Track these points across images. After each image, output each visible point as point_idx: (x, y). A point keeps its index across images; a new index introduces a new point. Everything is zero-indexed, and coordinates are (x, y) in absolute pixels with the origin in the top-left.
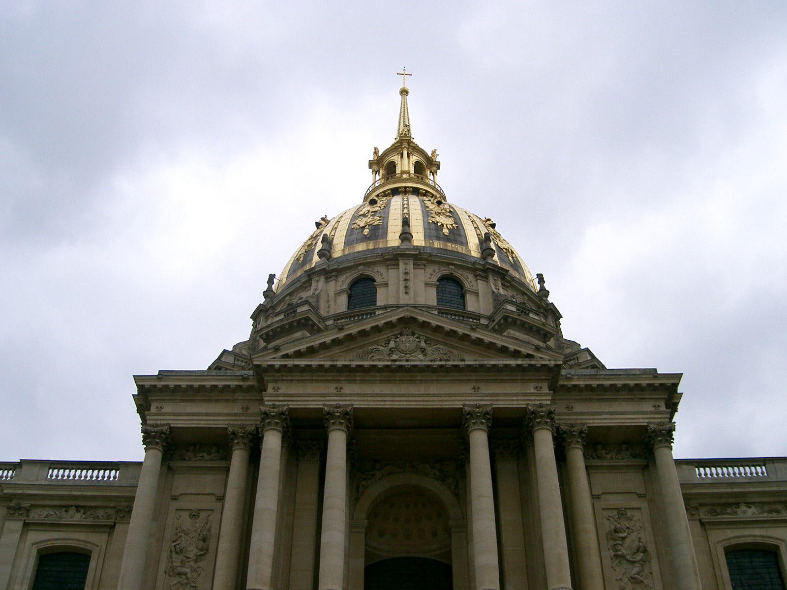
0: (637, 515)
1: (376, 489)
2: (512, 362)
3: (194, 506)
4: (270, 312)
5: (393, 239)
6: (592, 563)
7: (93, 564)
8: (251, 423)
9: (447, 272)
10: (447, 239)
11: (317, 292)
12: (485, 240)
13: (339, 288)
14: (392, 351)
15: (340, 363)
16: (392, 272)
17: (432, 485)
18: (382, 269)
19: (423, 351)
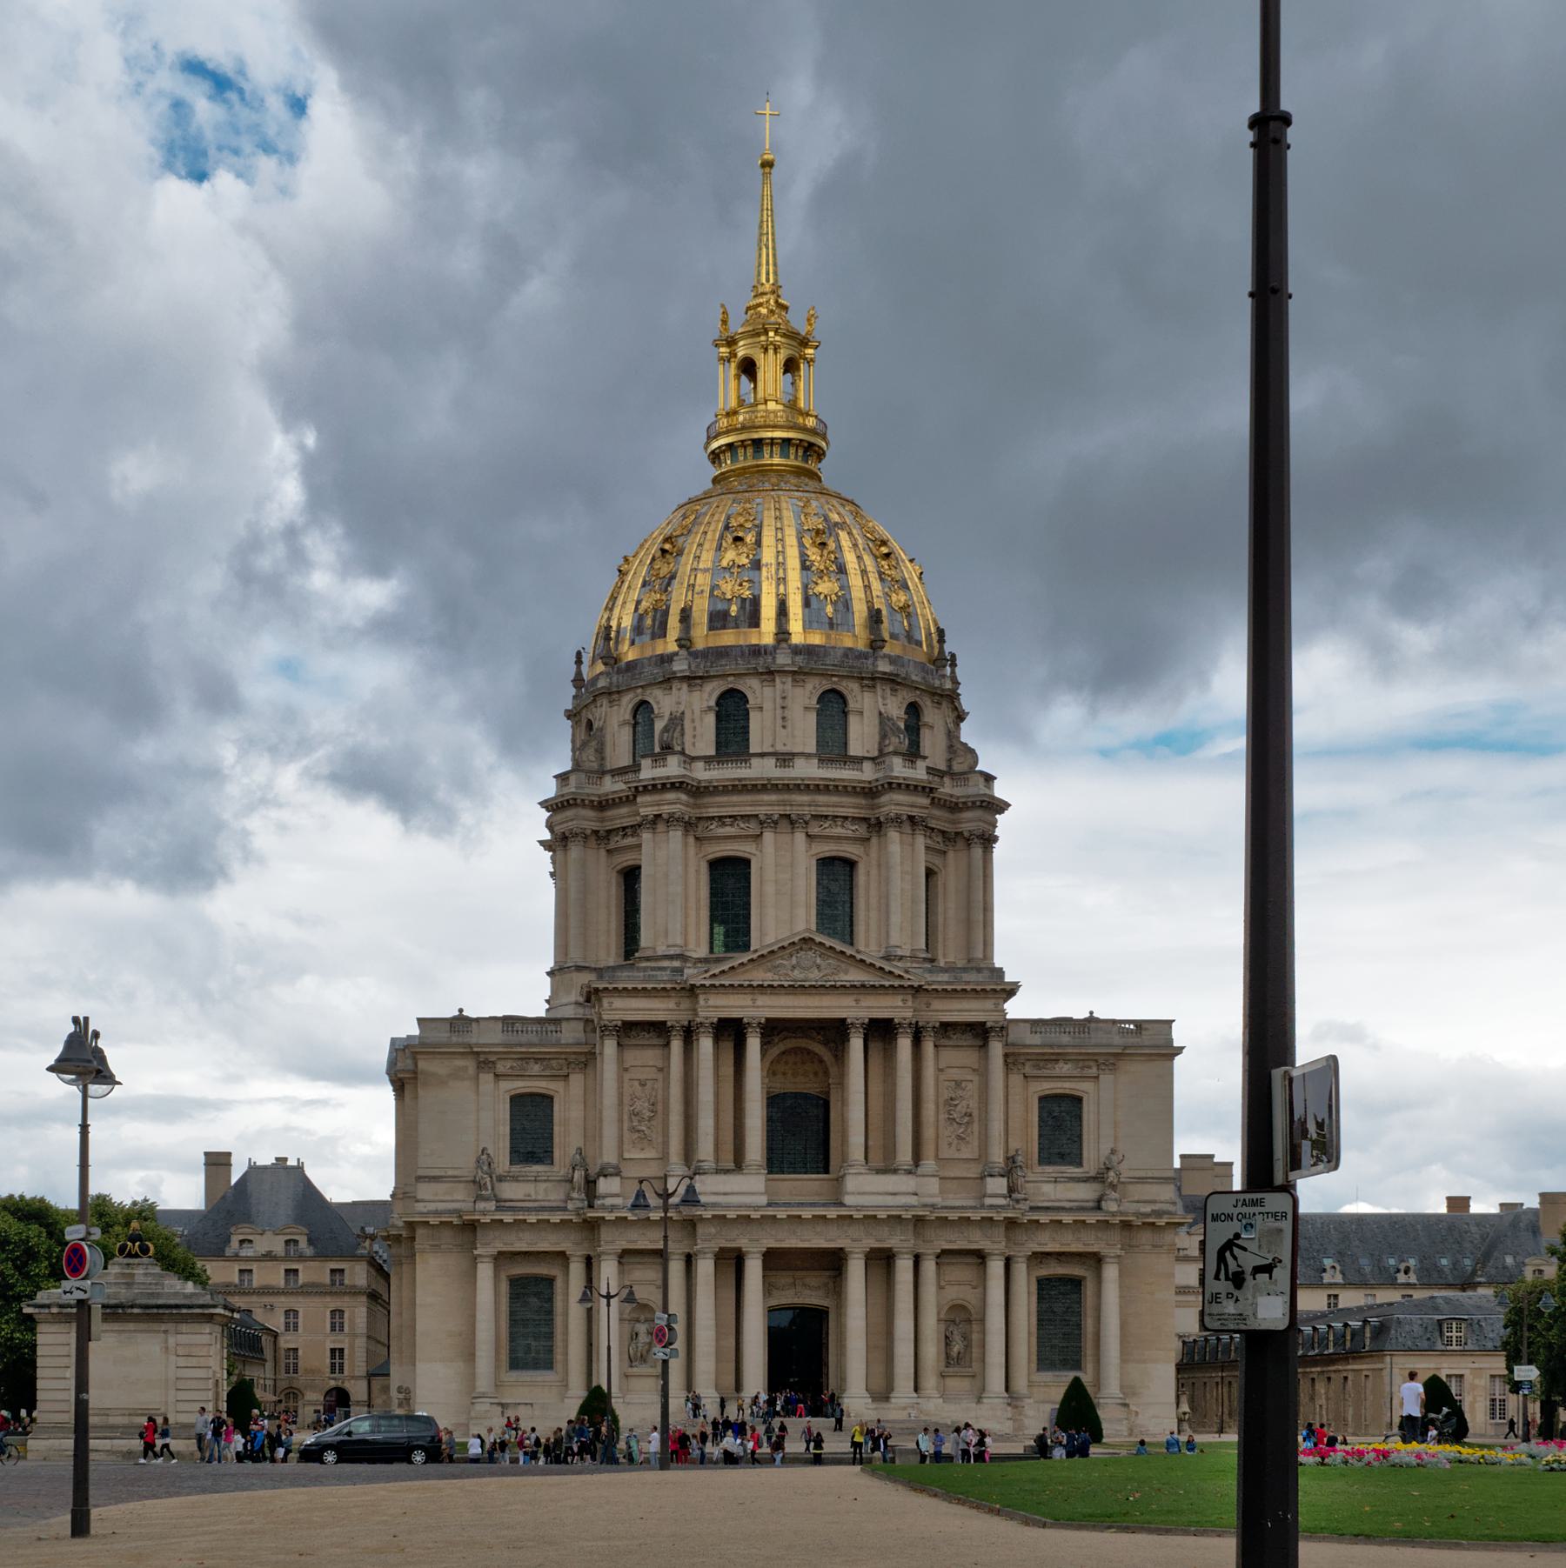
0: (970, 1086)
1: (775, 1051)
2: (887, 984)
3: (643, 1077)
4: (615, 696)
5: (767, 632)
6: (929, 1133)
7: (556, 1108)
8: (684, 1018)
9: (828, 687)
10: (831, 624)
11: (682, 708)
12: (875, 617)
13: (705, 705)
14: (794, 967)
15: (755, 984)
16: (768, 691)
17: (819, 1049)
18: (754, 683)
19: (818, 967)
